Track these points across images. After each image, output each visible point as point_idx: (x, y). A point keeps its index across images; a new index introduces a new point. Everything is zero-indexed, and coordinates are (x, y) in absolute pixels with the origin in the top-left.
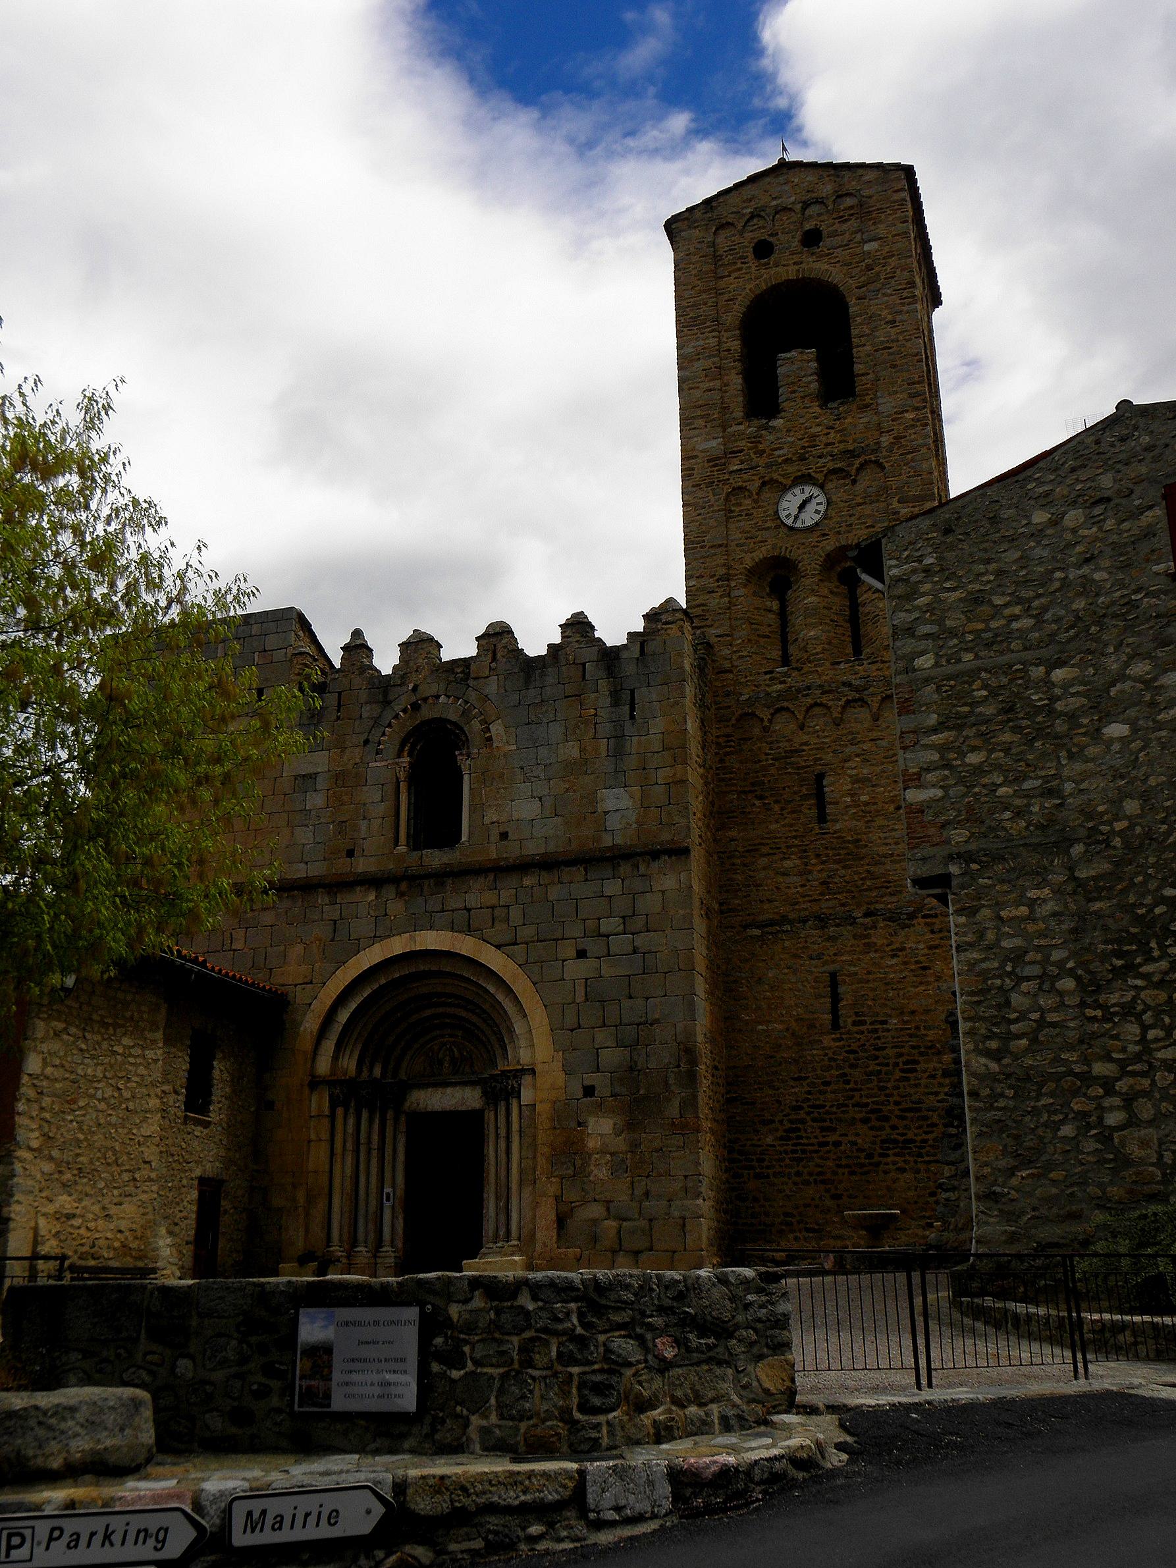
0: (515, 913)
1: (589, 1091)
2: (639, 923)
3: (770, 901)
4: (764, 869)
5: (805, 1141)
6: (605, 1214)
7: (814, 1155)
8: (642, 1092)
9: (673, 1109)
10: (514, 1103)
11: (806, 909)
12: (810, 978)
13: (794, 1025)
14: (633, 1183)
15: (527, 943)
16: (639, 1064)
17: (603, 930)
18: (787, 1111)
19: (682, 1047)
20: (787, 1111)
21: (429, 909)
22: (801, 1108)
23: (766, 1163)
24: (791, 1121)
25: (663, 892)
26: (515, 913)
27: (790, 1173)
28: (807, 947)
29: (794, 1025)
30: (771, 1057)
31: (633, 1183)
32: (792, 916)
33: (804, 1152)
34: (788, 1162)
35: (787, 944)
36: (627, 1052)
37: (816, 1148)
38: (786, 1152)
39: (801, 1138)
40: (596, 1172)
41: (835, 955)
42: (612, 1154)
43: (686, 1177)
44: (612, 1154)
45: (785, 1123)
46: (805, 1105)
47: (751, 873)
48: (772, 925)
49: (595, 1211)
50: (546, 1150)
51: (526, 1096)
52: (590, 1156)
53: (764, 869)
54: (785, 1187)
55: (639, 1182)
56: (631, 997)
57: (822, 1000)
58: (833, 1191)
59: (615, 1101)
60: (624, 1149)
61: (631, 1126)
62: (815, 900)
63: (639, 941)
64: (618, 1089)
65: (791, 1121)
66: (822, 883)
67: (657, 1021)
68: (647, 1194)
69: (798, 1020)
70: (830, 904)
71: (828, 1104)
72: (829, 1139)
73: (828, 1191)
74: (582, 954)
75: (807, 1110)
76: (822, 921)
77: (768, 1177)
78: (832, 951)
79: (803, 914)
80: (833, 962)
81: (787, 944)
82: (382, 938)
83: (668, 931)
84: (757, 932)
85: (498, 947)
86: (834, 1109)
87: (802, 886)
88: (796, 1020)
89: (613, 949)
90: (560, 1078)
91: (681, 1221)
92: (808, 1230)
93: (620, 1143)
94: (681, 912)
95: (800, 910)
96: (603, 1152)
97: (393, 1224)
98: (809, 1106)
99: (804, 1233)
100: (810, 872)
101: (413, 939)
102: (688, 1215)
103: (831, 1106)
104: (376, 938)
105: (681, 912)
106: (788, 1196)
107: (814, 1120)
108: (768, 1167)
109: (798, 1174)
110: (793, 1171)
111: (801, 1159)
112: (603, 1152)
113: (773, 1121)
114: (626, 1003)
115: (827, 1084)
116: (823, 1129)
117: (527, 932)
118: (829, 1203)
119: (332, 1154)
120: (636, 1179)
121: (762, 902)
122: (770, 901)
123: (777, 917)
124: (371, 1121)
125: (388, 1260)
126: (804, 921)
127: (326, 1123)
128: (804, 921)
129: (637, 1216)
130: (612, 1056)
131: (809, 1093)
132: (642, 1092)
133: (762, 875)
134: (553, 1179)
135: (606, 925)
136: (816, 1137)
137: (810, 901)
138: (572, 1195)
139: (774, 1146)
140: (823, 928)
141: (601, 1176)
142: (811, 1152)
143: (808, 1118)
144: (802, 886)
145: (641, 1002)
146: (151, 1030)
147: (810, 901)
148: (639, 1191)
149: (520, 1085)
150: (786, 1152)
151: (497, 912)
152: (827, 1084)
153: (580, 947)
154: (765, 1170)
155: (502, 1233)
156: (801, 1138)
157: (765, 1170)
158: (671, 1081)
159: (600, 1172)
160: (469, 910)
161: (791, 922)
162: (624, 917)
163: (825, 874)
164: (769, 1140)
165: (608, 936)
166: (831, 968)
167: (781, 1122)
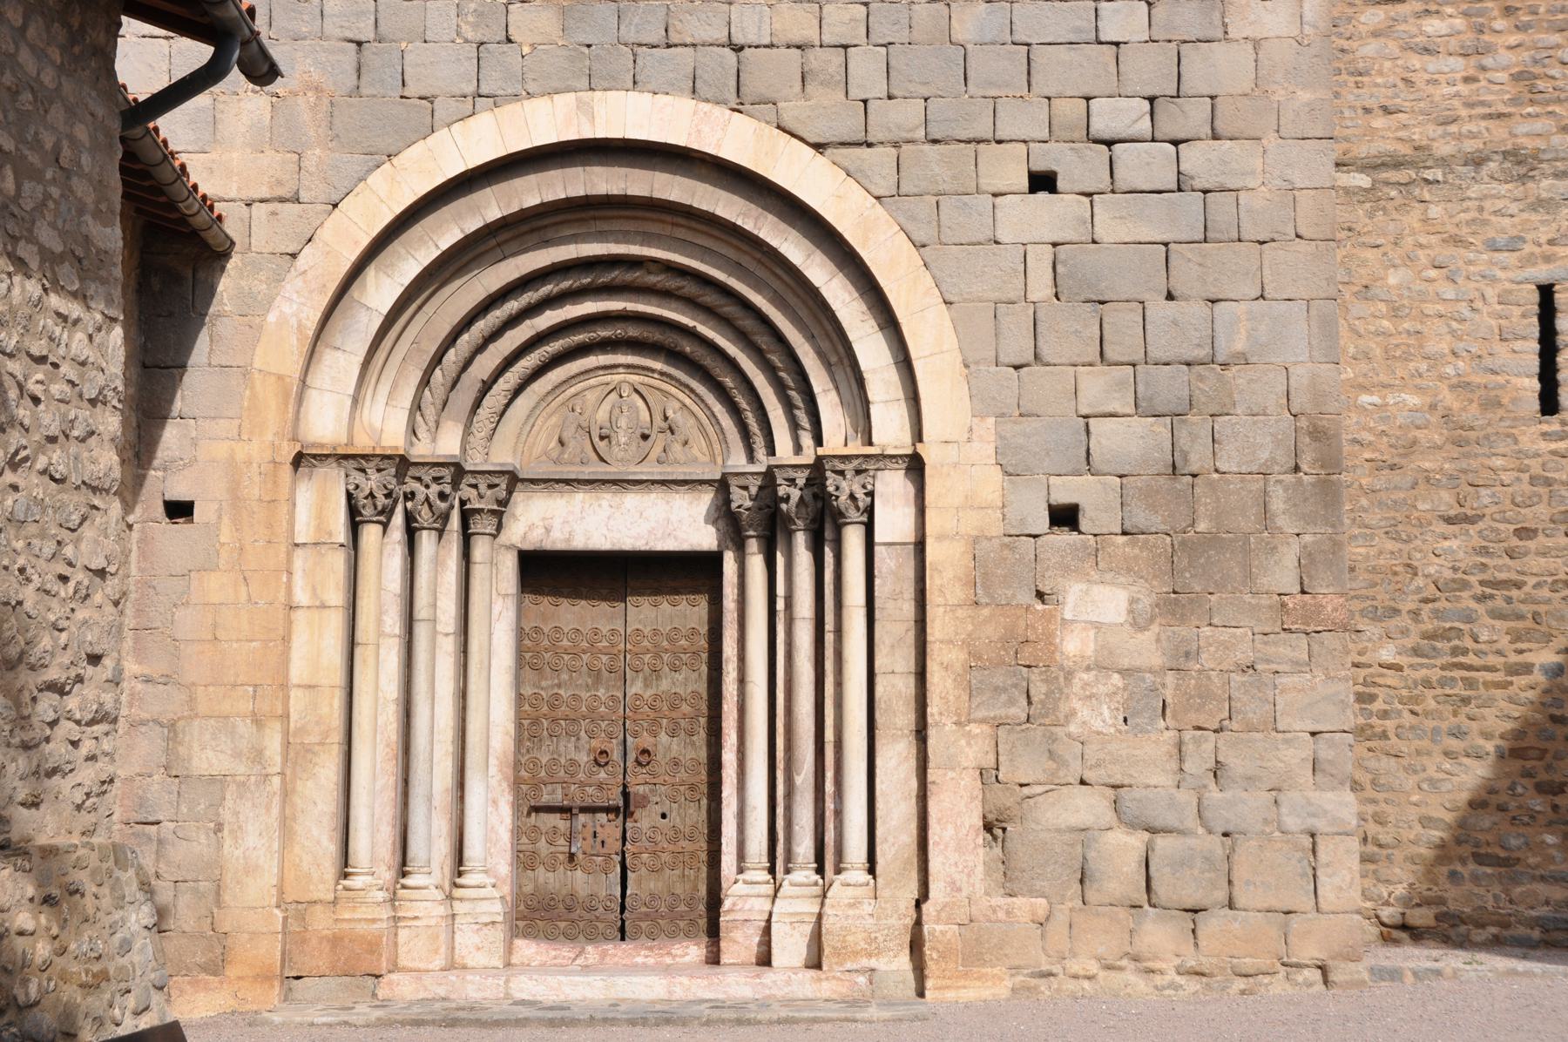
0: (867, 69)
1: (1065, 517)
2: (1193, 117)
3: (1386, 110)
4: (1376, 34)
5: (1470, 659)
6: (1109, 817)
7: (1498, 693)
8: (1202, 526)
9: (1282, 574)
10: (853, 539)
11: (1473, 136)
12: (1491, 293)
13: (1448, 399)
14: (1180, 745)
15: (896, 145)
16: (1193, 457)
17: (1100, 127)
18: (1431, 591)
19: (1303, 423)
20: (1431, 591)
21: (632, 37)
22: (1465, 585)
23: (1378, 705)
24: (1437, 614)
25: (1257, 44)
26: (867, 69)
27: (1436, 731)
28: (1485, 222)
29: (1448, 399)
30: (1392, 467)
31: (1180, 745)
32: (1444, 149)
33: (1470, 684)
34: (1432, 704)
35: (1435, 211)
36: (1161, 428)
37: (1499, 677)
38: (1427, 684)
39: (1465, 652)
40: (1084, 713)
41: (1551, 242)
42: (1124, 672)
43: (1313, 734)
44: (1124, 672)
45: (1424, 615)
46: (1473, 579)
47: (1345, 44)
48: (1398, 164)
49: (1087, 807)
50: (956, 656)
51: (894, 521)
52: (1069, 675)
53: (1376, 34)
54: (1425, 760)
55: (1198, 742)
56: (1170, 297)
57: (1518, 345)
58: (1543, 776)
59: (1133, 544)
60: (1157, 660)
61: (1176, 604)
62: (1500, 116)
63: (1195, 158)
64: (1140, 517)
65: (1437, 614)
66: (1517, 77)
67: (1244, 360)
68: (1217, 771)
69: (1461, 386)
70: (1539, 126)
71: (1532, 581)
72: (1528, 658)
73: (1528, 774)
74: (1042, 182)
75: (1479, 590)
76: (1522, 163)
77: (1384, 735)
78: (1544, 235)
79: (1470, 146)
80: (1548, 259)
81: (1435, 211)
82: (495, 100)
83: (1271, 141)
84: (1362, 180)
85: (819, 147)
86: (1545, 593)
87: (1467, 80)
88: (1453, 387)
89: (1125, 177)
90: (990, 483)
91: (1307, 842)
92: (1480, 859)
93: (1146, 649)
94: (1304, 96)
95: (1459, 137)
96: (1100, 667)
97: (492, 818)
98: (1482, 583)
99: (1472, 866)
100: (1488, 50)
101: (587, 111)
102: (1320, 825)
103: (1537, 586)
104: (480, 98)
105: (1304, 96)
106: (1431, 781)
107: (1497, 615)
108: (1385, 715)
109: (1457, 733)
110: (1444, 726)
111: (1466, 701)
112: (1100, 667)
113: (1396, 612)
114: (1159, 310)
115: (1524, 533)
116: (1517, 637)
117: (904, 116)
118: (1538, 803)
119: (352, 643)
120: (1188, 735)
121: (1367, 111)
122: (1386, 110)
123: (1405, 150)
124: (437, 562)
125: (484, 907)
126: (1477, 161)
127: (338, 562)
128: (1477, 161)
129: (1191, 821)
130: (1127, 439)
131: (1484, 551)
132: (1202, 526)
133: (1370, 48)
134: (975, 729)
135: (1113, 116)
136: (1499, 653)
137: (1490, 116)
138: (1024, 766)
139: (1397, 668)
140: (1523, 179)
141: (1097, 725)
142: (1486, 684)
143: (1480, 609)
144: (1467, 80)
145: (1198, 309)
146: (97, 214)
147: (1490, 116)
148: (1198, 764)
149: (871, 494)
150: (1427, 684)
151: (816, 58)
152: (1524, 533)
153: (1040, 166)
154: (1374, 720)
155: (804, 847)
156: (1465, 652)
157: (1374, 720)
158: (1278, 504)
159: (1093, 715)
160: (738, 49)
161: (1443, 162)
162: (1152, 100)
163: (1526, 56)
164: (1387, 654)
165: (1109, 143)
166: (1543, 273)
167: (1415, 614)
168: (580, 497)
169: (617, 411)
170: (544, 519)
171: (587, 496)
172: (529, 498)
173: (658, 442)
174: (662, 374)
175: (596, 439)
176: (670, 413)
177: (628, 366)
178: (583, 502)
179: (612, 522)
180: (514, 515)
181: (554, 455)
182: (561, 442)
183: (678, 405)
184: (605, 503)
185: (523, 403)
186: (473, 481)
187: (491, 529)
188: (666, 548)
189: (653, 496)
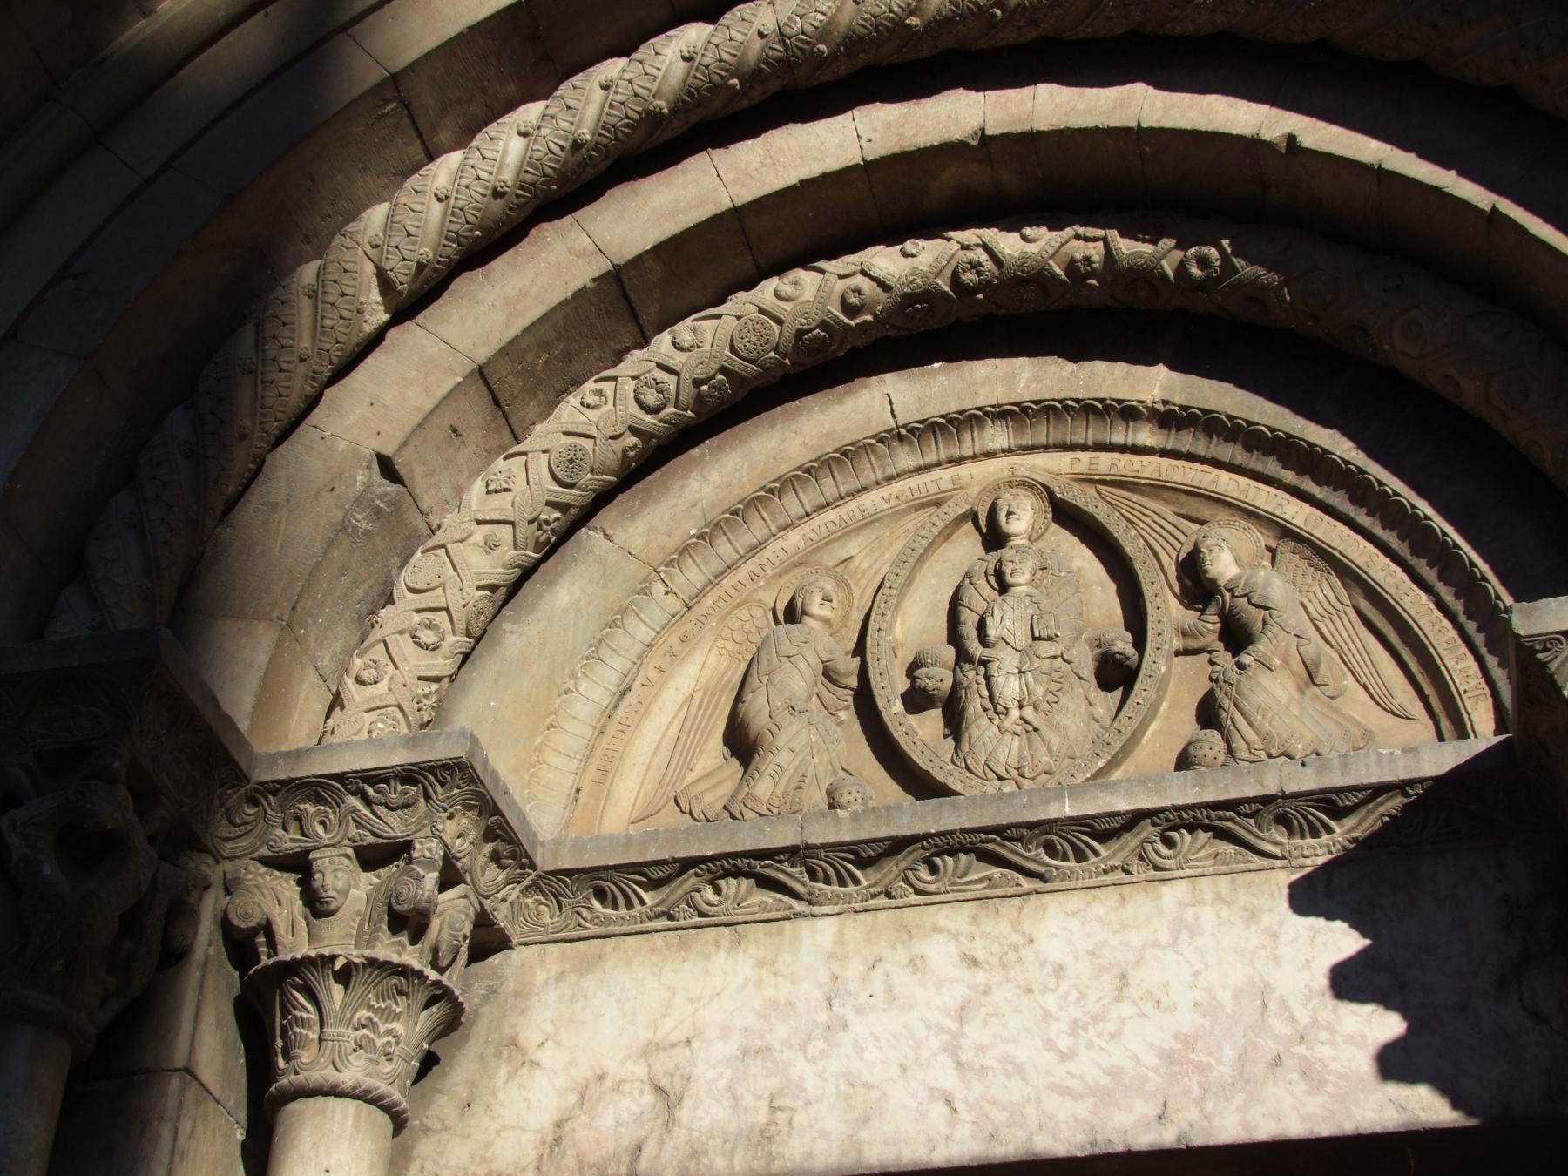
168: (820, 942)
169: (980, 596)
170: (651, 1049)
171: (856, 927)
172: (586, 966)
173: (1173, 685)
174: (1169, 418)
175: (892, 709)
176: (1223, 566)
177: (1014, 414)
178: (837, 955)
179: (975, 1033)
180: (513, 1043)
181: (713, 799)
182: (742, 743)
183: (1255, 539)
184: (940, 952)
185: (568, 593)
186: (287, 841)
187: (387, 1078)
188: (1265, 1129)
189: (1173, 894)
